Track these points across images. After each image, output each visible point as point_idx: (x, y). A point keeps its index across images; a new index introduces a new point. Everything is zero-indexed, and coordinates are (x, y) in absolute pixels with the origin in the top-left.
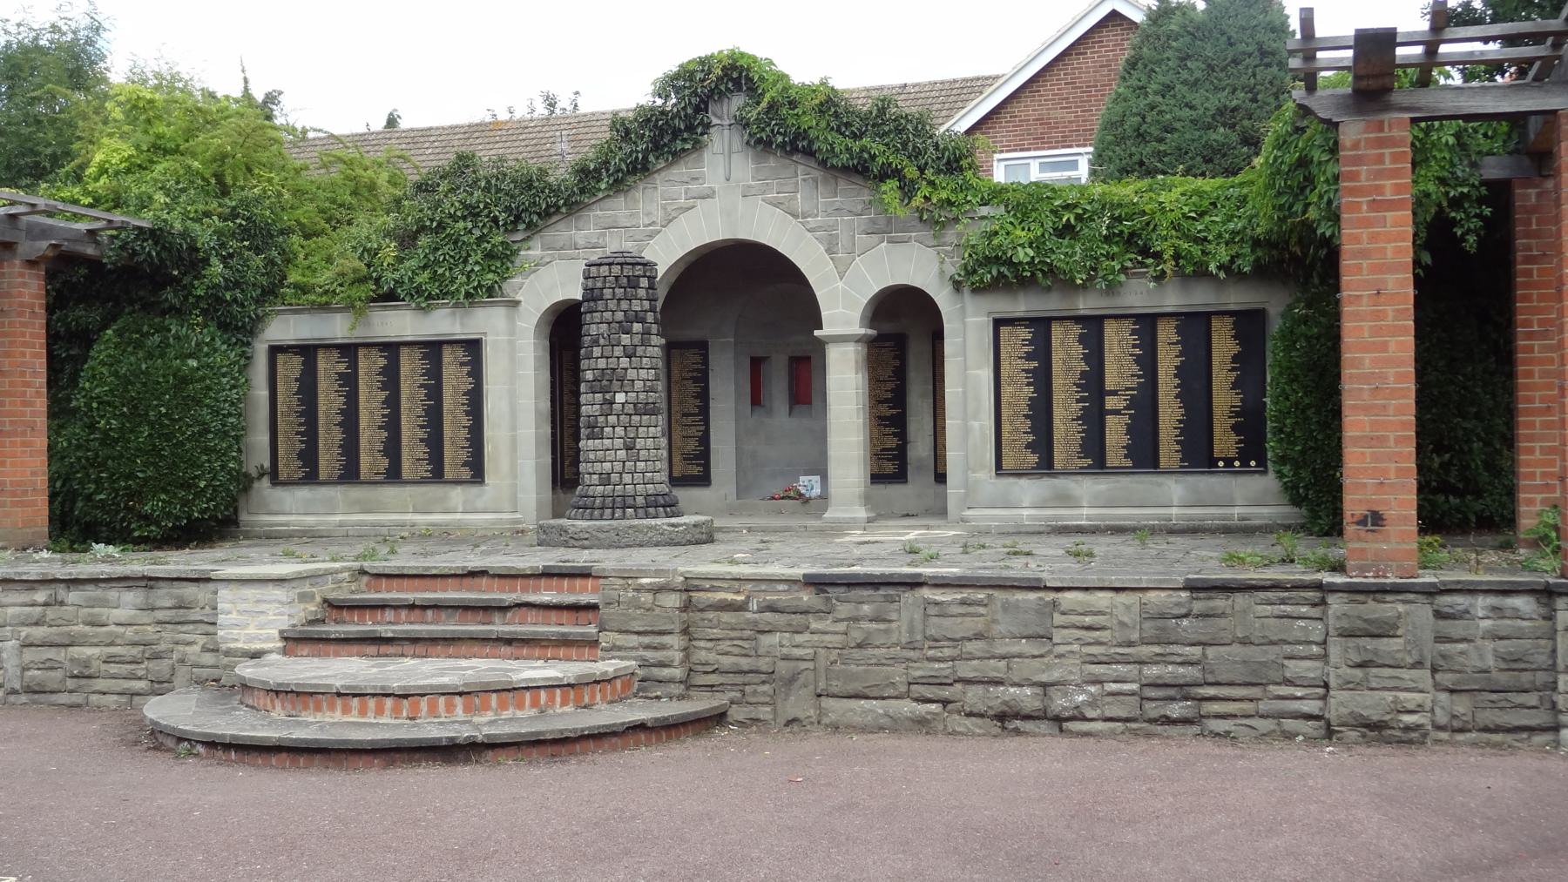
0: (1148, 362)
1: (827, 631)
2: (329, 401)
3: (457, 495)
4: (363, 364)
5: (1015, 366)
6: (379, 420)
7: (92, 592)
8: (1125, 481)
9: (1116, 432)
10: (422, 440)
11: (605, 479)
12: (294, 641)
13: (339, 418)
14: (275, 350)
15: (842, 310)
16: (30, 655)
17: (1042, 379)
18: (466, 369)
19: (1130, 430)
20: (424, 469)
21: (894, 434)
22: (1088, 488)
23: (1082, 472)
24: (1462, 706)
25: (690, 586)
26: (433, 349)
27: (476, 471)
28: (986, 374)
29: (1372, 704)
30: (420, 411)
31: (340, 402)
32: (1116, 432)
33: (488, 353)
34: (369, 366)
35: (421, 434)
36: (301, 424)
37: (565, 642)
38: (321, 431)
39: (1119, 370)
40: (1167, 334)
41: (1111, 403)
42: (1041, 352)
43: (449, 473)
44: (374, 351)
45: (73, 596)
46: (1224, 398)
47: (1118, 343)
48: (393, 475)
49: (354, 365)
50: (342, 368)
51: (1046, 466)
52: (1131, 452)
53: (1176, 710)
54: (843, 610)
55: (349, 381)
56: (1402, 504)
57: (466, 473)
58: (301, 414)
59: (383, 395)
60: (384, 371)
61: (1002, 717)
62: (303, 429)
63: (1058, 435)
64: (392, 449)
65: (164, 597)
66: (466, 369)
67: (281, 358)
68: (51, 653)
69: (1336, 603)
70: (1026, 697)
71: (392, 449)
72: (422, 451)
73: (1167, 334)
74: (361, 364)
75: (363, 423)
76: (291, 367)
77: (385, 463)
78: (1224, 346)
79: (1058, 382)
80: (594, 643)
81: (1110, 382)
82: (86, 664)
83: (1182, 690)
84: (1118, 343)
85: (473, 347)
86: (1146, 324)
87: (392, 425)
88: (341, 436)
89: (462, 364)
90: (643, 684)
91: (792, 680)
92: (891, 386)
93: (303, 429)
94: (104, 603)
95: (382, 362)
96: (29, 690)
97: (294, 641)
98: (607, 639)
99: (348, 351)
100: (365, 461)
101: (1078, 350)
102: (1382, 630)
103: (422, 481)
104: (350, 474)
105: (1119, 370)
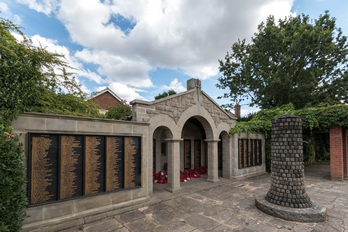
2: (67, 159)
3: (131, 193)
6: (95, 167)
10: (115, 174)
13: (74, 168)
14: (31, 136)
18: (134, 147)
20: (116, 185)
21: (189, 160)
26: (121, 138)
30: (115, 163)
33: (143, 140)
34: (91, 146)
35: (115, 172)
36: (48, 173)
38: (62, 175)
44: (94, 139)
48: (103, 190)
49: (83, 144)
50: (76, 145)
55: (81, 151)
57: (133, 184)
58: (49, 168)
59: (98, 157)
60: (98, 147)
62: (50, 175)
66: (134, 147)
67: (35, 139)
72: (115, 179)
73: (253, 141)
74: (87, 144)
75: (87, 170)
77: (98, 185)
85: (138, 140)
87: (103, 169)
88: (74, 177)
89: (132, 145)
92: (189, 150)
93: (50, 175)
95: (98, 143)
99: (81, 138)
100: (87, 186)
103: (115, 190)
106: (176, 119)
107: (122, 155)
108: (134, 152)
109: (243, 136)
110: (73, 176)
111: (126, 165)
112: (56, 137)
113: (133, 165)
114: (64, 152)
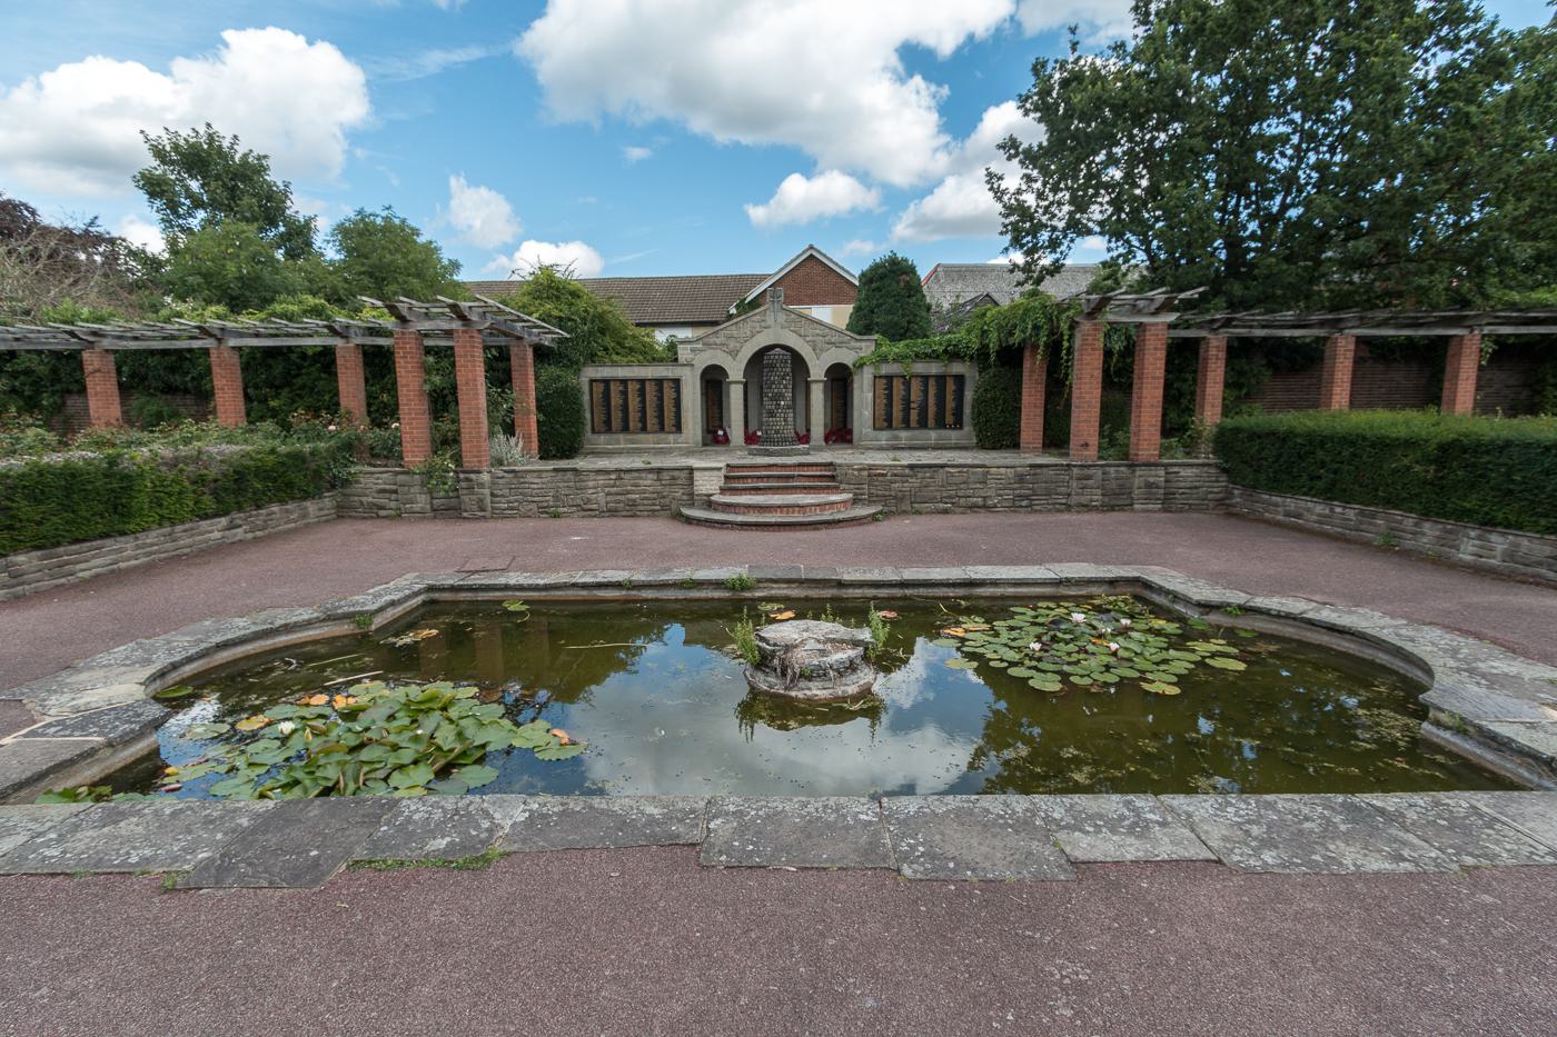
0: (926, 392)
1: (914, 482)
2: (616, 400)
3: (671, 437)
4: (630, 387)
5: (881, 392)
7: (636, 474)
8: (917, 432)
9: (914, 415)
11: (777, 432)
12: (723, 491)
14: (592, 381)
15: (817, 371)
16: (609, 498)
17: (890, 397)
19: (919, 415)
20: (657, 427)
22: (904, 434)
23: (904, 428)
24: (1106, 499)
25: (871, 467)
26: (659, 382)
27: (678, 428)
28: (870, 395)
29: (1084, 500)
31: (621, 402)
32: (914, 415)
33: (683, 384)
34: (633, 388)
37: (828, 488)
39: (916, 395)
40: (932, 382)
41: (913, 405)
42: (890, 387)
43: (667, 429)
45: (627, 476)
46: (950, 404)
47: (916, 386)
48: (644, 429)
49: (626, 387)
50: (621, 388)
51: (890, 427)
52: (919, 422)
53: (1024, 503)
54: (920, 475)
55: (625, 393)
56: (1094, 440)
57: (674, 429)
60: (639, 390)
61: (970, 507)
63: (895, 415)
64: (643, 420)
65: (666, 476)
68: (619, 497)
69: (1075, 470)
70: (980, 501)
71: (643, 420)
72: (655, 421)
73: (932, 382)
75: (631, 409)
76: (599, 388)
78: (951, 387)
79: (895, 398)
80: (837, 488)
81: (913, 398)
82: (634, 501)
83: (1027, 497)
84: (916, 386)
85: (677, 382)
86: (925, 378)
87: (643, 411)
90: (855, 501)
91: (902, 499)
94: (641, 478)
95: (638, 386)
96: (609, 511)
97: (723, 491)
98: (842, 486)
99: (624, 382)
100: (631, 424)
101: (902, 387)
102: (1089, 477)
104: (625, 429)
105: (916, 395)
106: (734, 353)
107: (661, 399)
108: (674, 395)
109: (885, 369)
110: (620, 414)
111: (666, 409)
112: (606, 382)
113: (674, 409)
114: (613, 395)
